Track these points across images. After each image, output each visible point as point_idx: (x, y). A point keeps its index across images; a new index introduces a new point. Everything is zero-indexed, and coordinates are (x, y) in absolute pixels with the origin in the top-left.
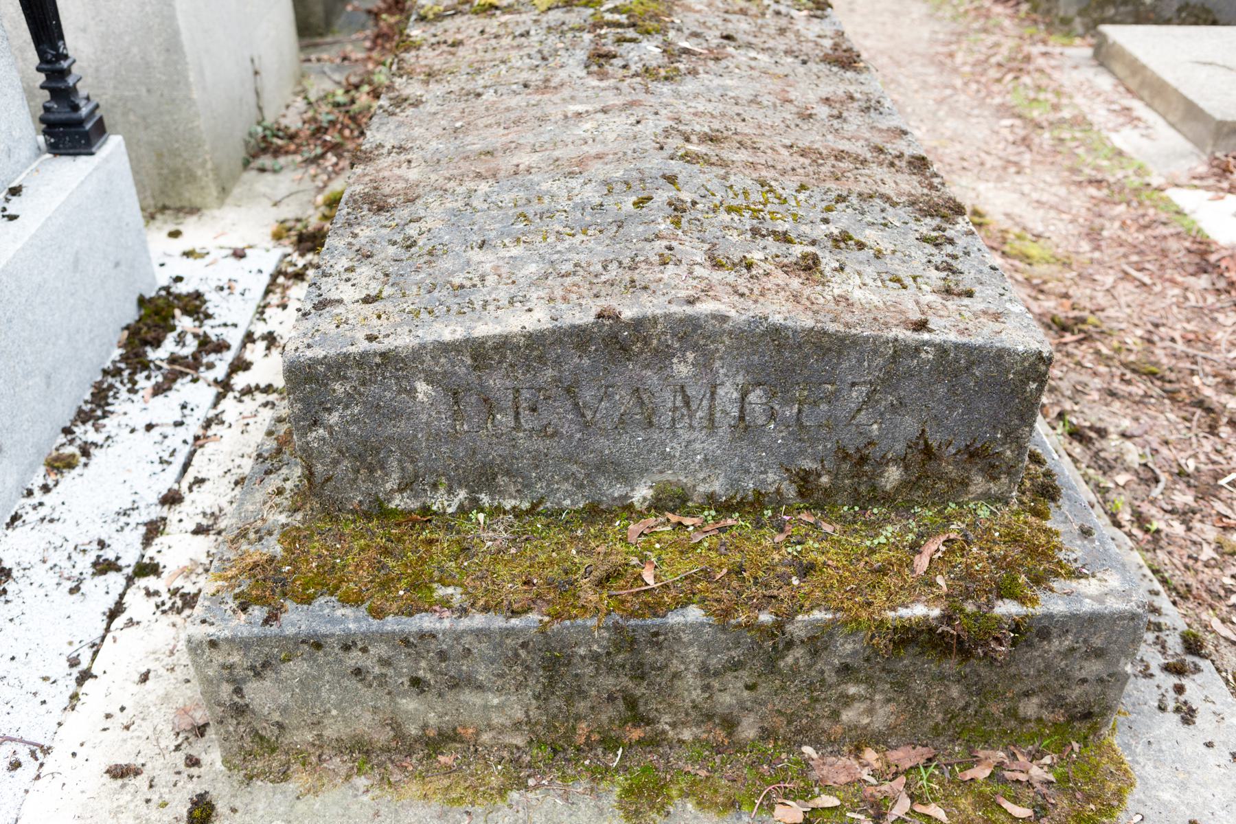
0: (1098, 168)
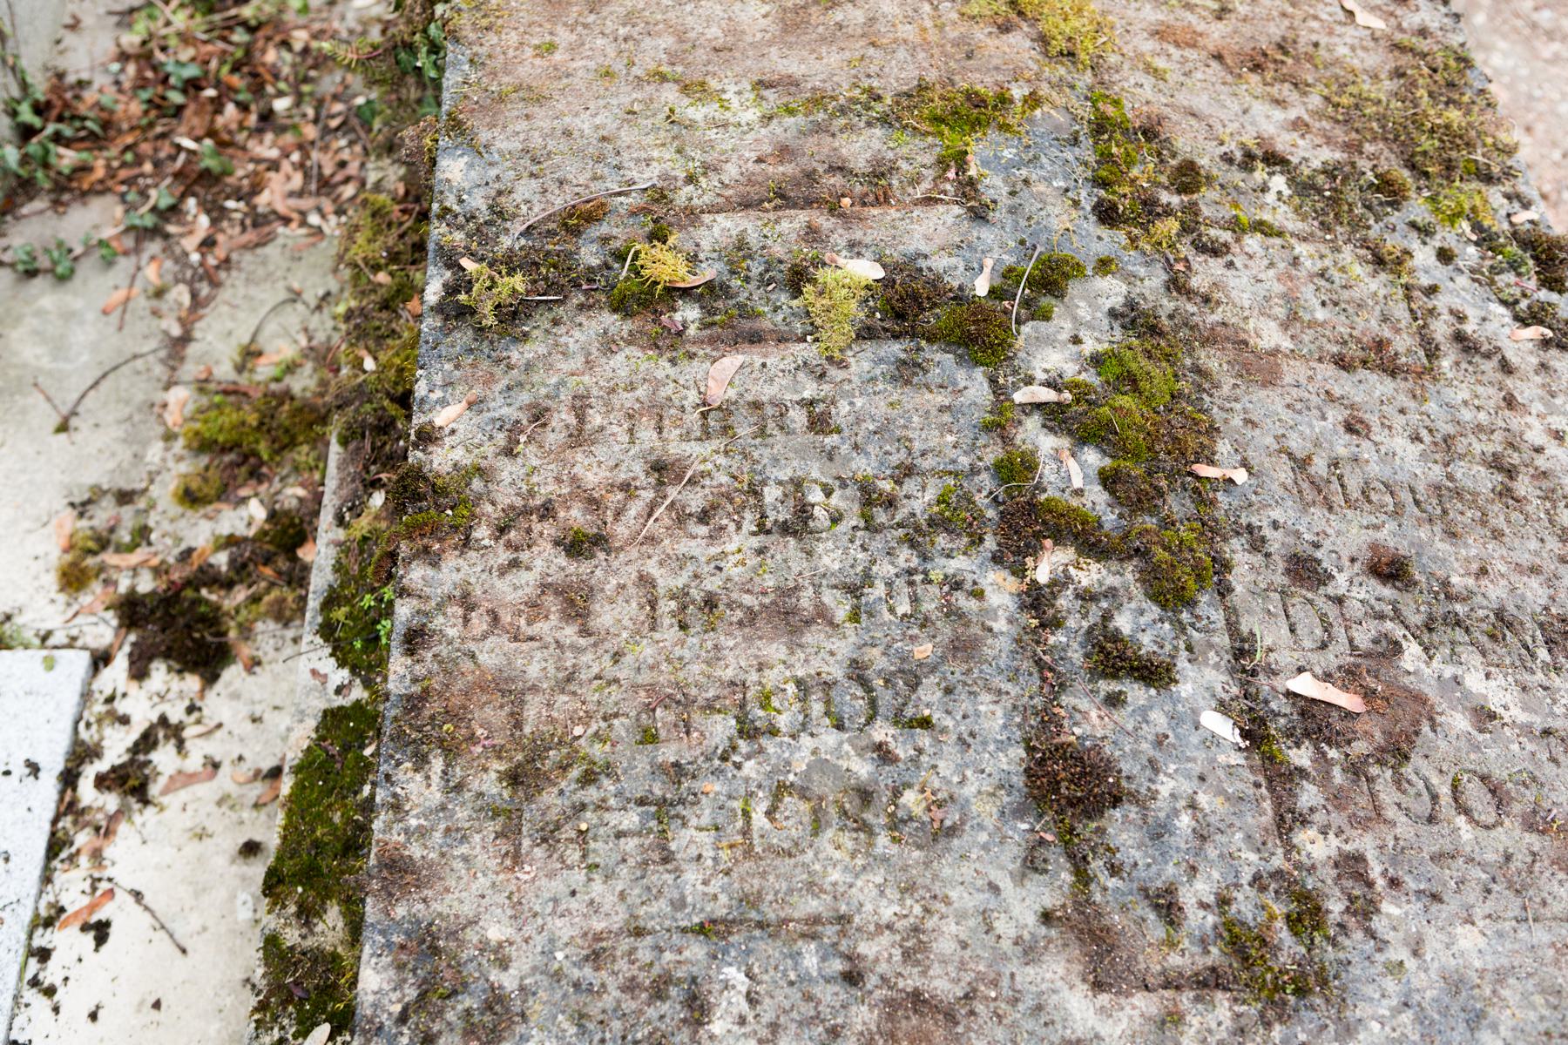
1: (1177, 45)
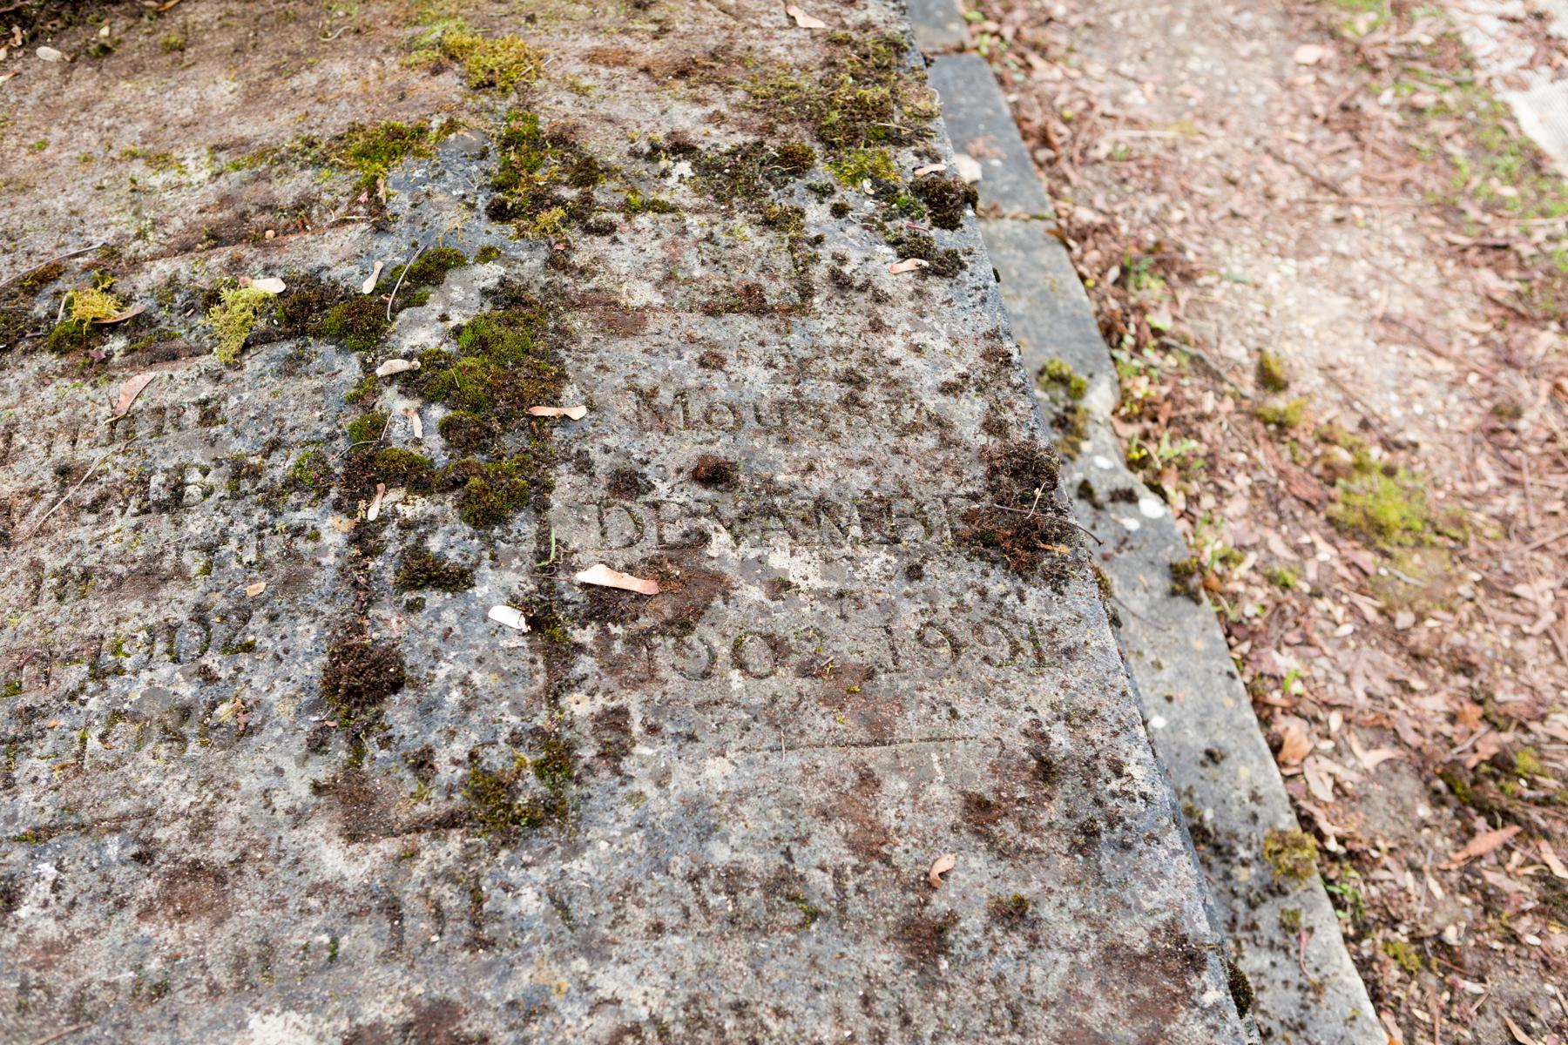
0: (1493, 206)
1: (607, 64)
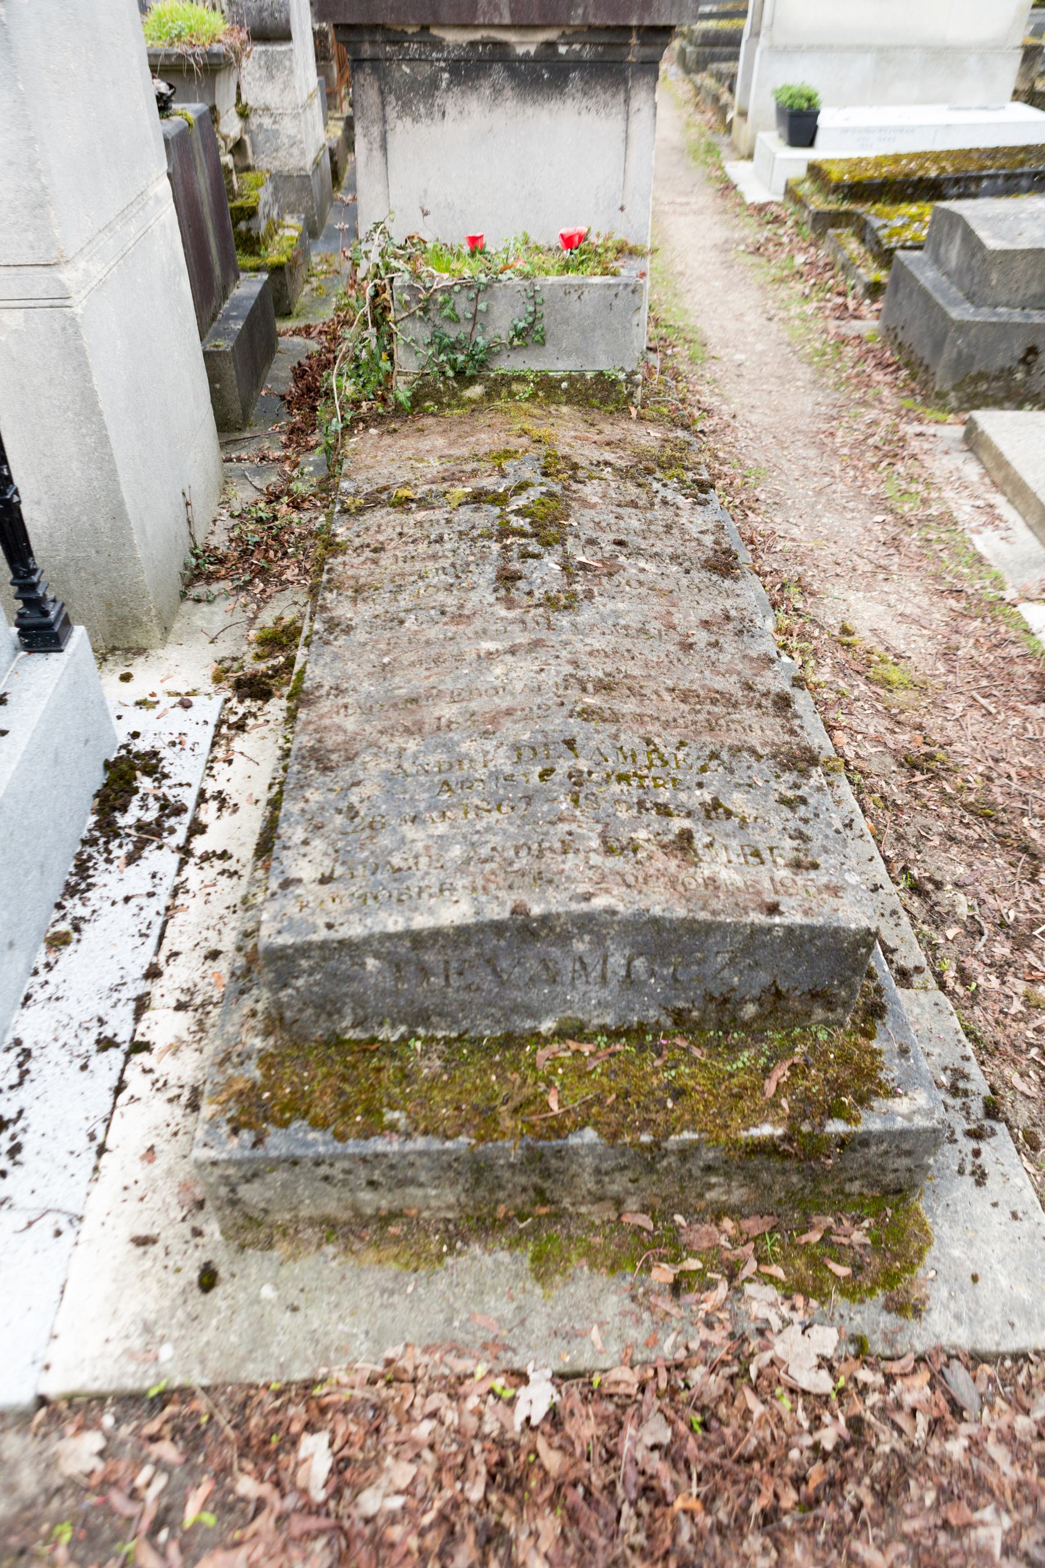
0: (958, 576)
